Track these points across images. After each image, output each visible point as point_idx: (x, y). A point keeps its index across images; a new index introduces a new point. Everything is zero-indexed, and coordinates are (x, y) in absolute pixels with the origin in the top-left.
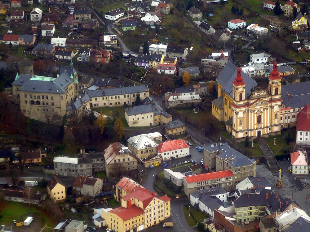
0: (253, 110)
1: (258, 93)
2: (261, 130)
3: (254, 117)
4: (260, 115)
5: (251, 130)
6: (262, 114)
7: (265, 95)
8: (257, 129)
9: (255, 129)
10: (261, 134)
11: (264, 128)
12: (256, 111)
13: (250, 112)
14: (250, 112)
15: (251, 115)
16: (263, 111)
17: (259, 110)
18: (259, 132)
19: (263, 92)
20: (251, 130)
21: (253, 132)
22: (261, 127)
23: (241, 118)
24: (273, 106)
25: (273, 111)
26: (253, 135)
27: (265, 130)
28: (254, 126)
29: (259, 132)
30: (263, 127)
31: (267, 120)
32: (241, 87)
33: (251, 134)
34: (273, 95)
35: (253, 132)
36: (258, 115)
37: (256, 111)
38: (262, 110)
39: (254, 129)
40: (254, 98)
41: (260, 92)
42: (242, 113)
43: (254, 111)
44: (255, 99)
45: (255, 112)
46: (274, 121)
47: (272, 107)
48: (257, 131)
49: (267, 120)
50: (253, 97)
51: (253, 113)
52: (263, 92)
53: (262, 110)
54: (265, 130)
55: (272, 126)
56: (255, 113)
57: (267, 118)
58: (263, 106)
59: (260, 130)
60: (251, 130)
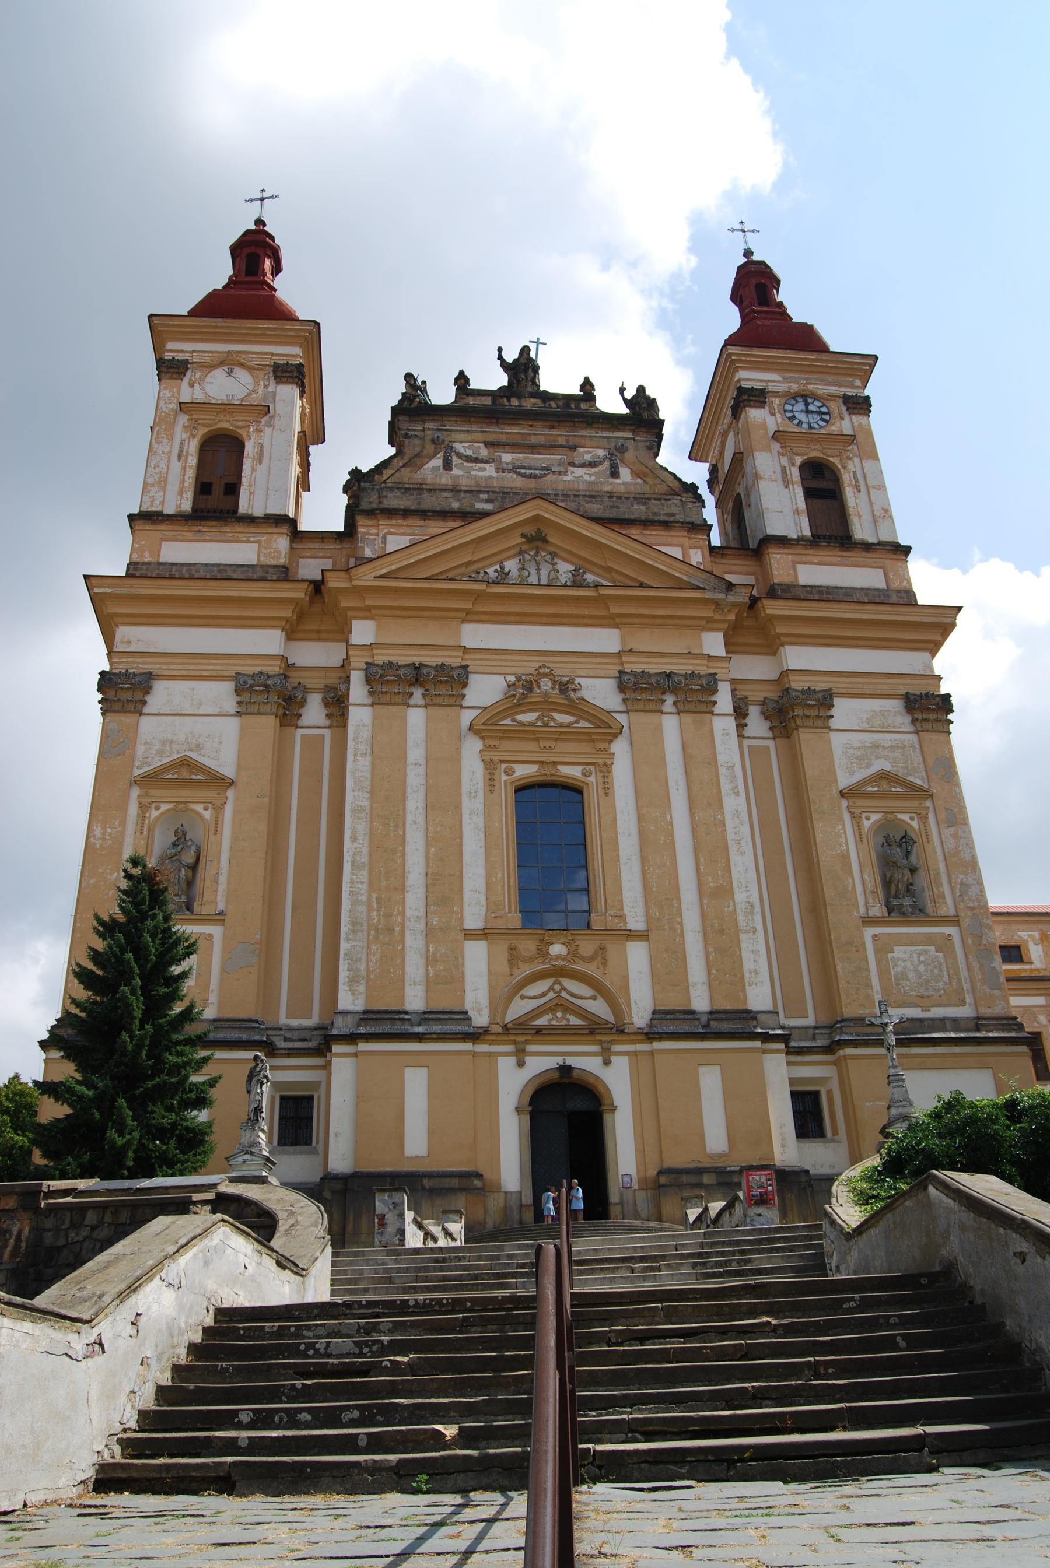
0: (432, 659)
1: (514, 446)
2: (616, 1077)
3: (444, 802)
4: (572, 772)
5: (368, 1016)
6: (606, 769)
7: (642, 499)
8: (521, 1034)
9: (480, 1019)
10: (626, 1156)
11: (673, 1024)
12: (485, 690)
13: (358, 690)
14: (358, 690)
15: (389, 754)
16: (622, 718)
17: (540, 690)
18: (568, 1123)
19: (586, 455)
20: (384, 1024)
21: (416, 1084)
22: (599, 1008)
23: (187, 775)
24: (798, 684)
25: (811, 767)
26: (416, 1145)
27: (710, 1082)
28: (447, 974)
29: (568, 1123)
30: (640, 1016)
31: (716, 892)
32: (229, 363)
33: (380, 1110)
34: (782, 541)
35: (416, 1084)
36: (524, 771)
37: (485, 690)
38: (600, 692)
39: (447, 1024)
40: (429, 502)
41: (551, 447)
42: (220, 694)
43: (442, 682)
44: (444, 514)
45: (457, 701)
46: (883, 948)
47: (793, 711)
48: (513, 1079)
49: (725, 891)
50: (420, 488)
51: (416, 718)
52: (586, 455)
53: (600, 692)
54: (710, 1082)
55: (839, 1035)
56: (467, 717)
57: (711, 850)
58: (605, 640)
59: (586, 1061)
60: (384, 1024)
